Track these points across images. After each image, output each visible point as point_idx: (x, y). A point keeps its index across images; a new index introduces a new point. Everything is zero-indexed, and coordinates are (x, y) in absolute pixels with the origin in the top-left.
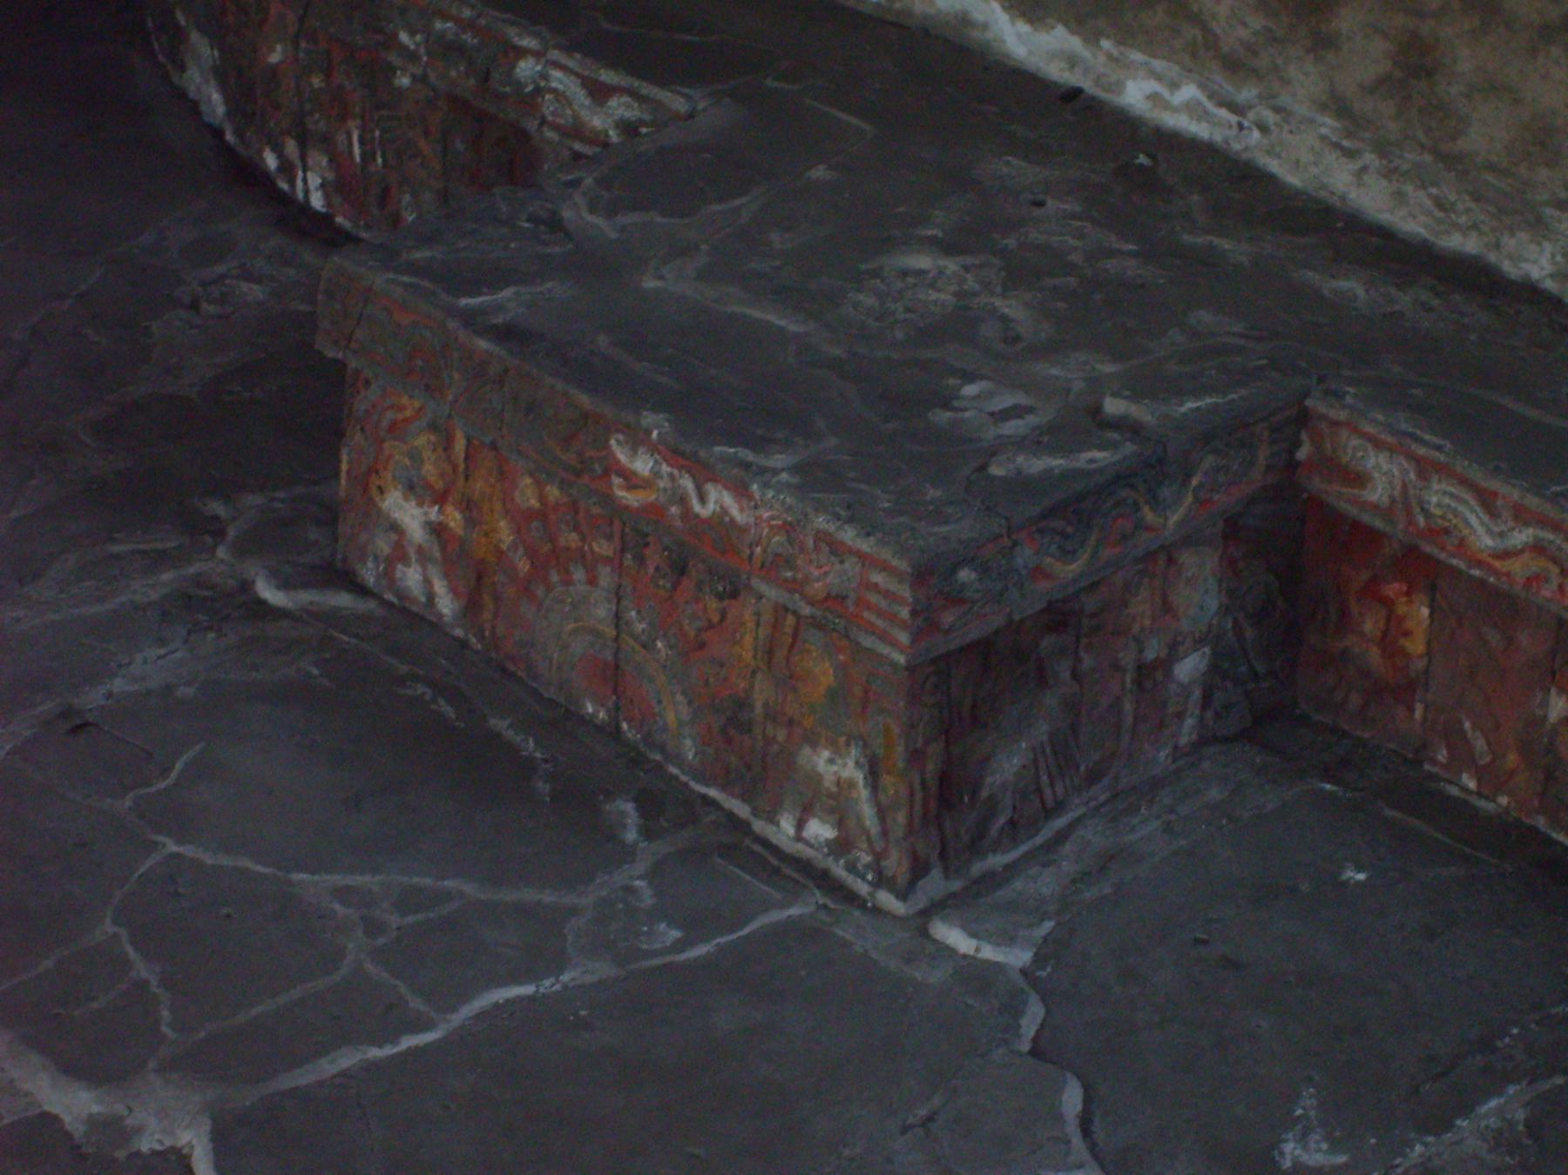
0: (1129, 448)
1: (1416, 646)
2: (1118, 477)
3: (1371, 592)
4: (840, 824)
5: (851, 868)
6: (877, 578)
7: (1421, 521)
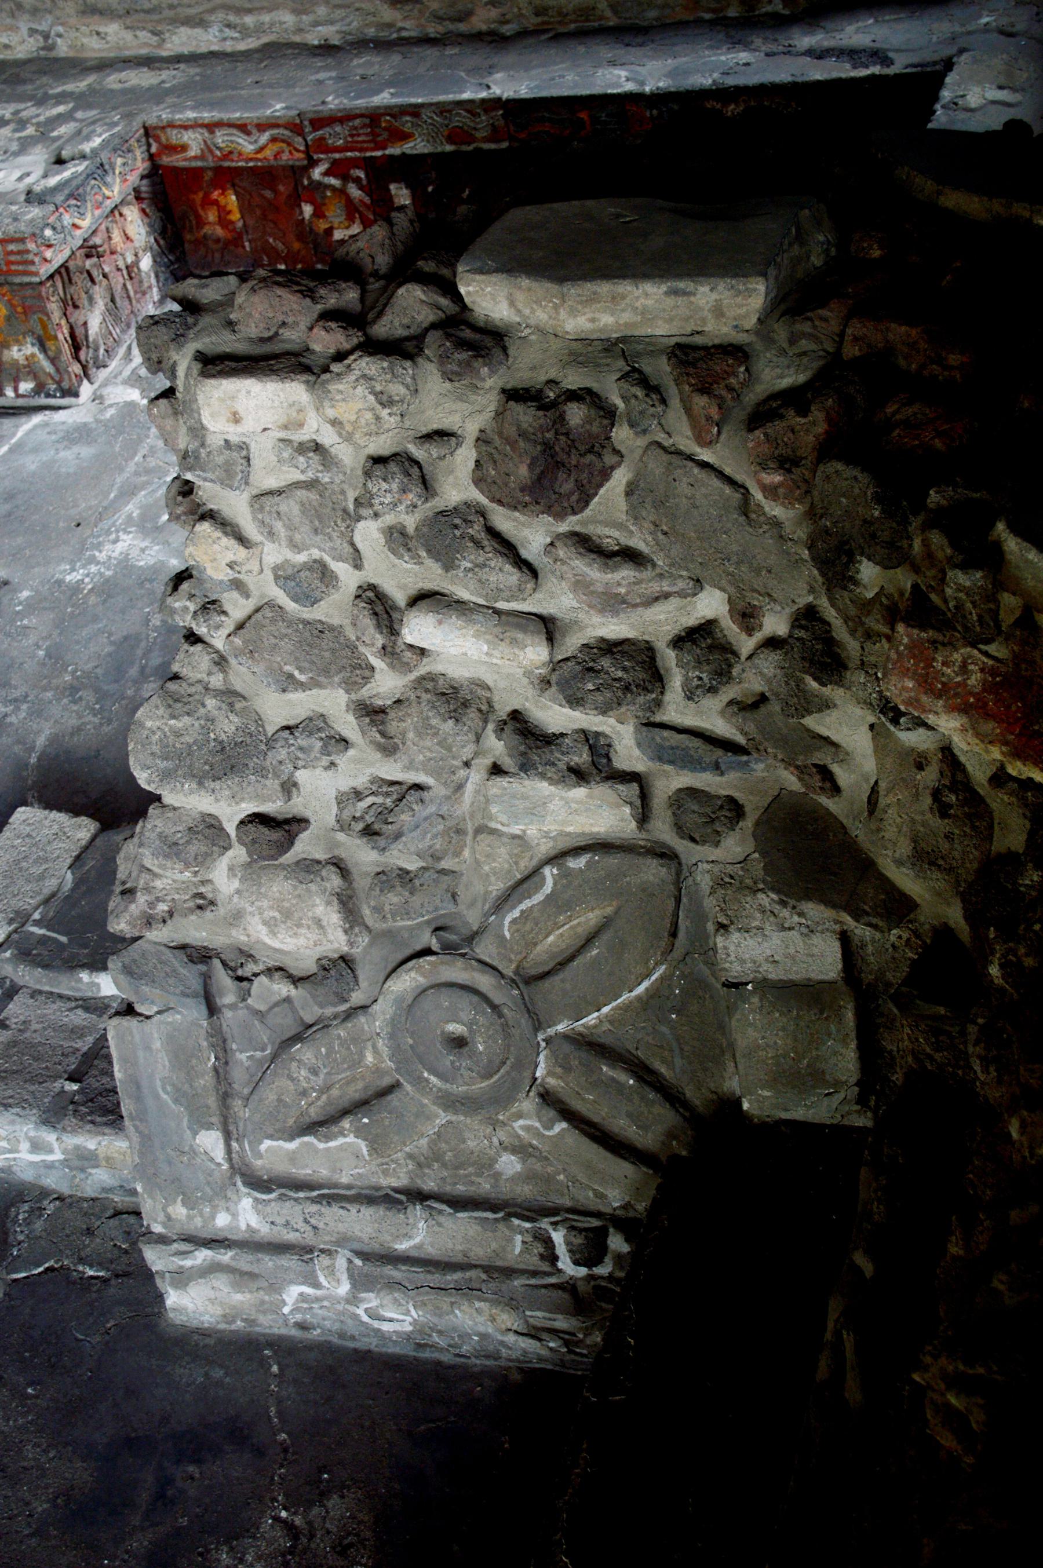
0: (86, 163)
1: (236, 216)
2: (88, 176)
3: (208, 202)
4: (35, 377)
5: (48, 395)
6: (12, 247)
7: (218, 153)
